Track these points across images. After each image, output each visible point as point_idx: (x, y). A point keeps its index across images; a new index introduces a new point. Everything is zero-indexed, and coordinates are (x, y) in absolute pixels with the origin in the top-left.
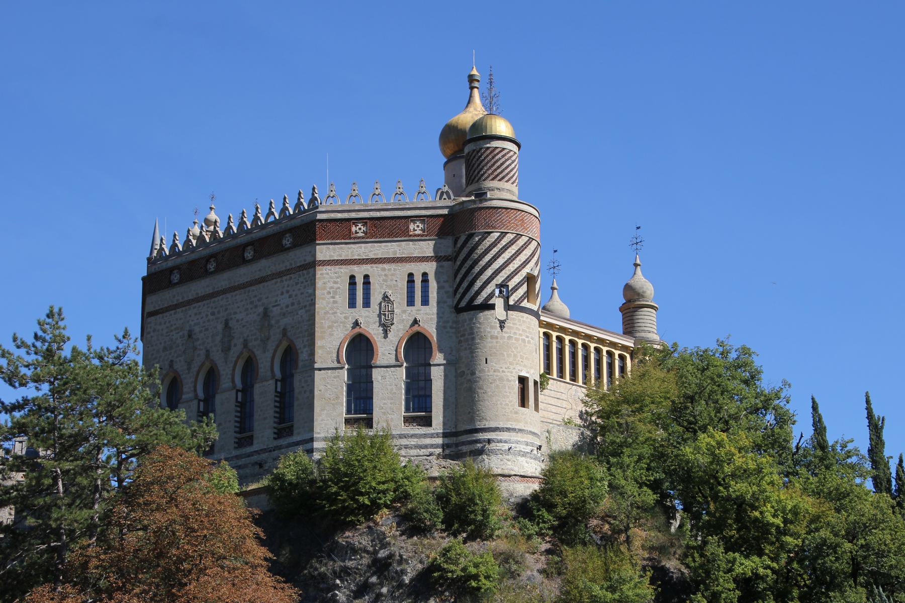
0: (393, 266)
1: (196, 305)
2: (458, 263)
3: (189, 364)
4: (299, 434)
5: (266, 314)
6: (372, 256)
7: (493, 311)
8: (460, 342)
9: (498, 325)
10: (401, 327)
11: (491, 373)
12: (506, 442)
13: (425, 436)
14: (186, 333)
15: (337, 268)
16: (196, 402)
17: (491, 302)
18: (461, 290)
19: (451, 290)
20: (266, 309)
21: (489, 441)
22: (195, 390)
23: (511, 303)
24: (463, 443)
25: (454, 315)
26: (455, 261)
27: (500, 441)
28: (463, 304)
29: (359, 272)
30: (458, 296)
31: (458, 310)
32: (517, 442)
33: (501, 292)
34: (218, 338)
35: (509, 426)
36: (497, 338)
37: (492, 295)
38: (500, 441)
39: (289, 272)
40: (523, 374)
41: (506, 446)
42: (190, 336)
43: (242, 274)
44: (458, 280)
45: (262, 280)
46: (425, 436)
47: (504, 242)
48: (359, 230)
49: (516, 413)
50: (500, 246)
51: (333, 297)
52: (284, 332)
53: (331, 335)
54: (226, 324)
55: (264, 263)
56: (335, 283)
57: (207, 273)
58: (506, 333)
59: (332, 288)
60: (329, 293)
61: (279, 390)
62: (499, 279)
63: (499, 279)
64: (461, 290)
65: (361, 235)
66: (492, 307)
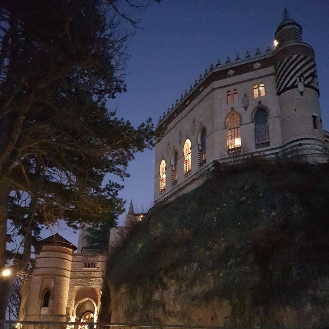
0: (247, 83)
1: (171, 131)
2: (277, 74)
3: (168, 154)
4: (208, 161)
5: (194, 122)
6: (237, 81)
7: (296, 89)
8: (281, 107)
9: (300, 94)
10: (252, 107)
11: (298, 115)
12: (309, 144)
13: (266, 150)
14: (167, 143)
15: (222, 89)
16: (171, 167)
17: (296, 84)
18: (280, 84)
19: (275, 87)
20: (194, 119)
21: (300, 145)
22: (171, 163)
23: (306, 83)
24: (287, 149)
25: (277, 97)
26: (276, 73)
27: (305, 144)
28: (282, 89)
29: (231, 88)
30: (278, 87)
31: (279, 94)
32: (314, 144)
33: (300, 81)
34: (178, 140)
35: (310, 137)
36: (300, 99)
37: (296, 81)
38: (305, 144)
39: (202, 99)
40: (315, 114)
41: (309, 146)
42: (168, 144)
43: (187, 110)
44: (278, 81)
45: (193, 108)
46: (266, 150)
47: (299, 59)
48: (231, 72)
49: (313, 131)
50: (297, 61)
51: (220, 101)
52: (201, 125)
53: (220, 117)
54: (180, 133)
55: (193, 102)
56: (221, 95)
57: (174, 118)
58: (304, 97)
59: (220, 98)
60: (219, 100)
61: (200, 148)
62: (299, 74)
63: (299, 74)
64: (280, 84)
65: (232, 74)
66: (297, 86)
